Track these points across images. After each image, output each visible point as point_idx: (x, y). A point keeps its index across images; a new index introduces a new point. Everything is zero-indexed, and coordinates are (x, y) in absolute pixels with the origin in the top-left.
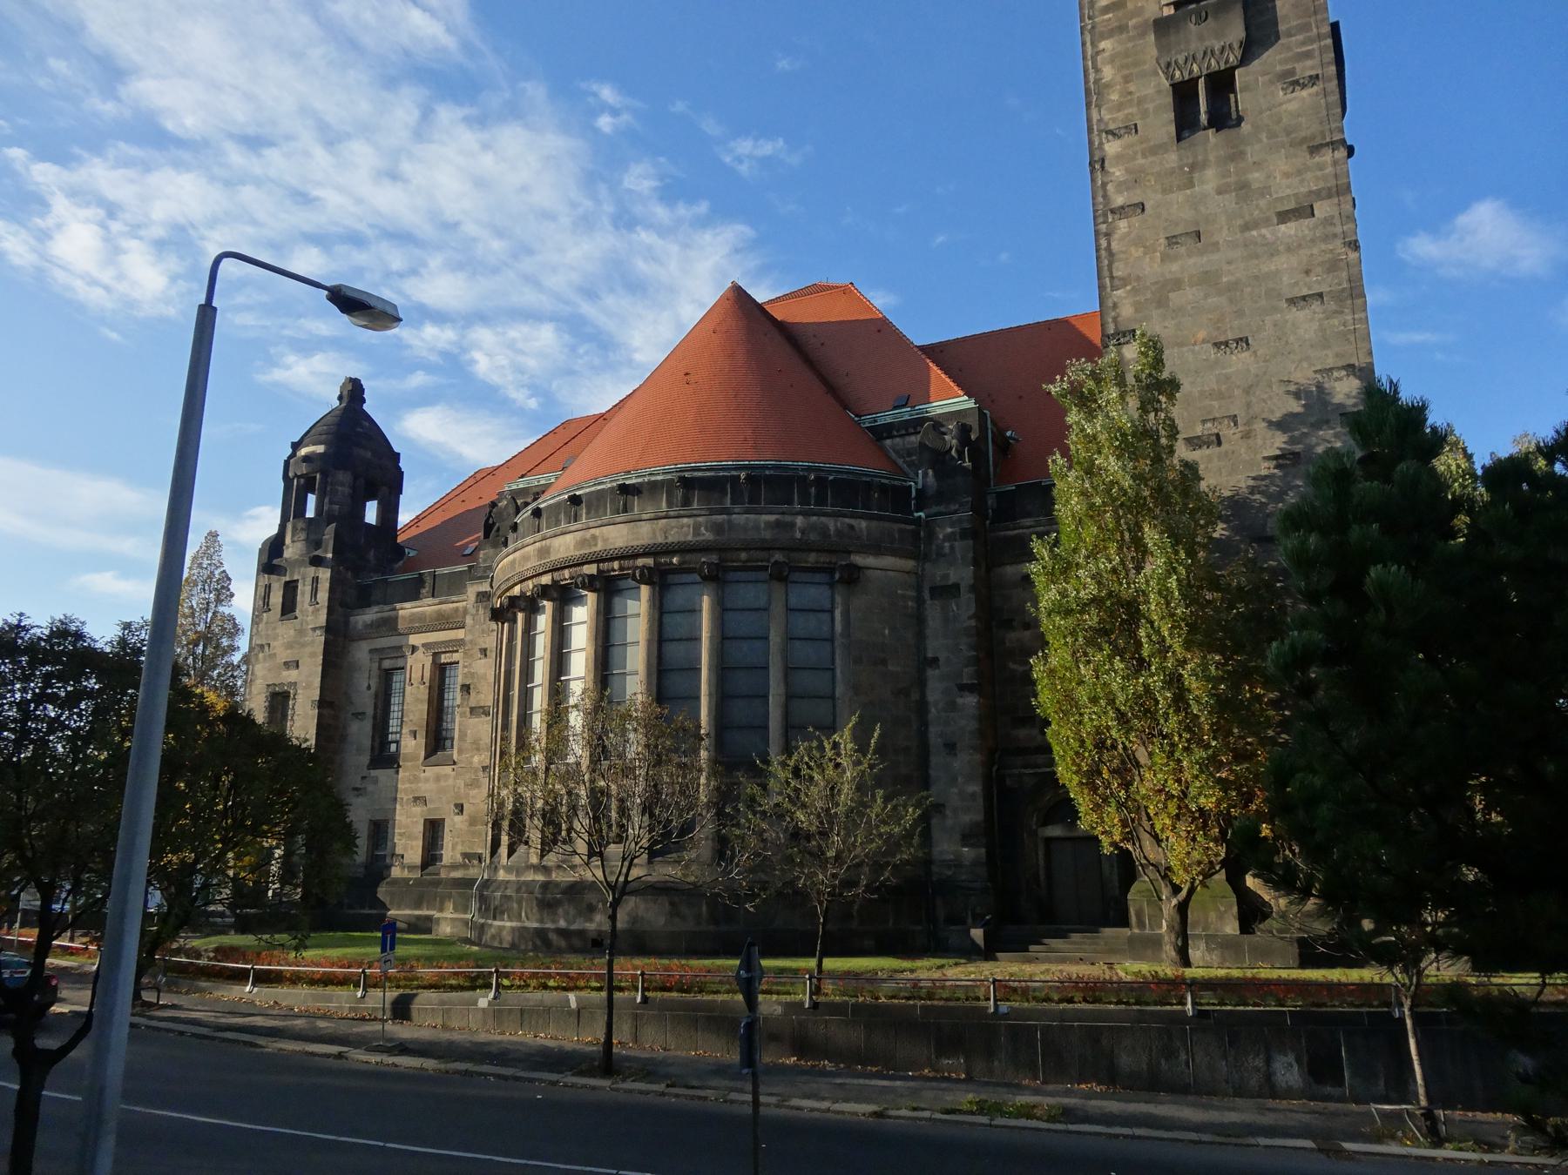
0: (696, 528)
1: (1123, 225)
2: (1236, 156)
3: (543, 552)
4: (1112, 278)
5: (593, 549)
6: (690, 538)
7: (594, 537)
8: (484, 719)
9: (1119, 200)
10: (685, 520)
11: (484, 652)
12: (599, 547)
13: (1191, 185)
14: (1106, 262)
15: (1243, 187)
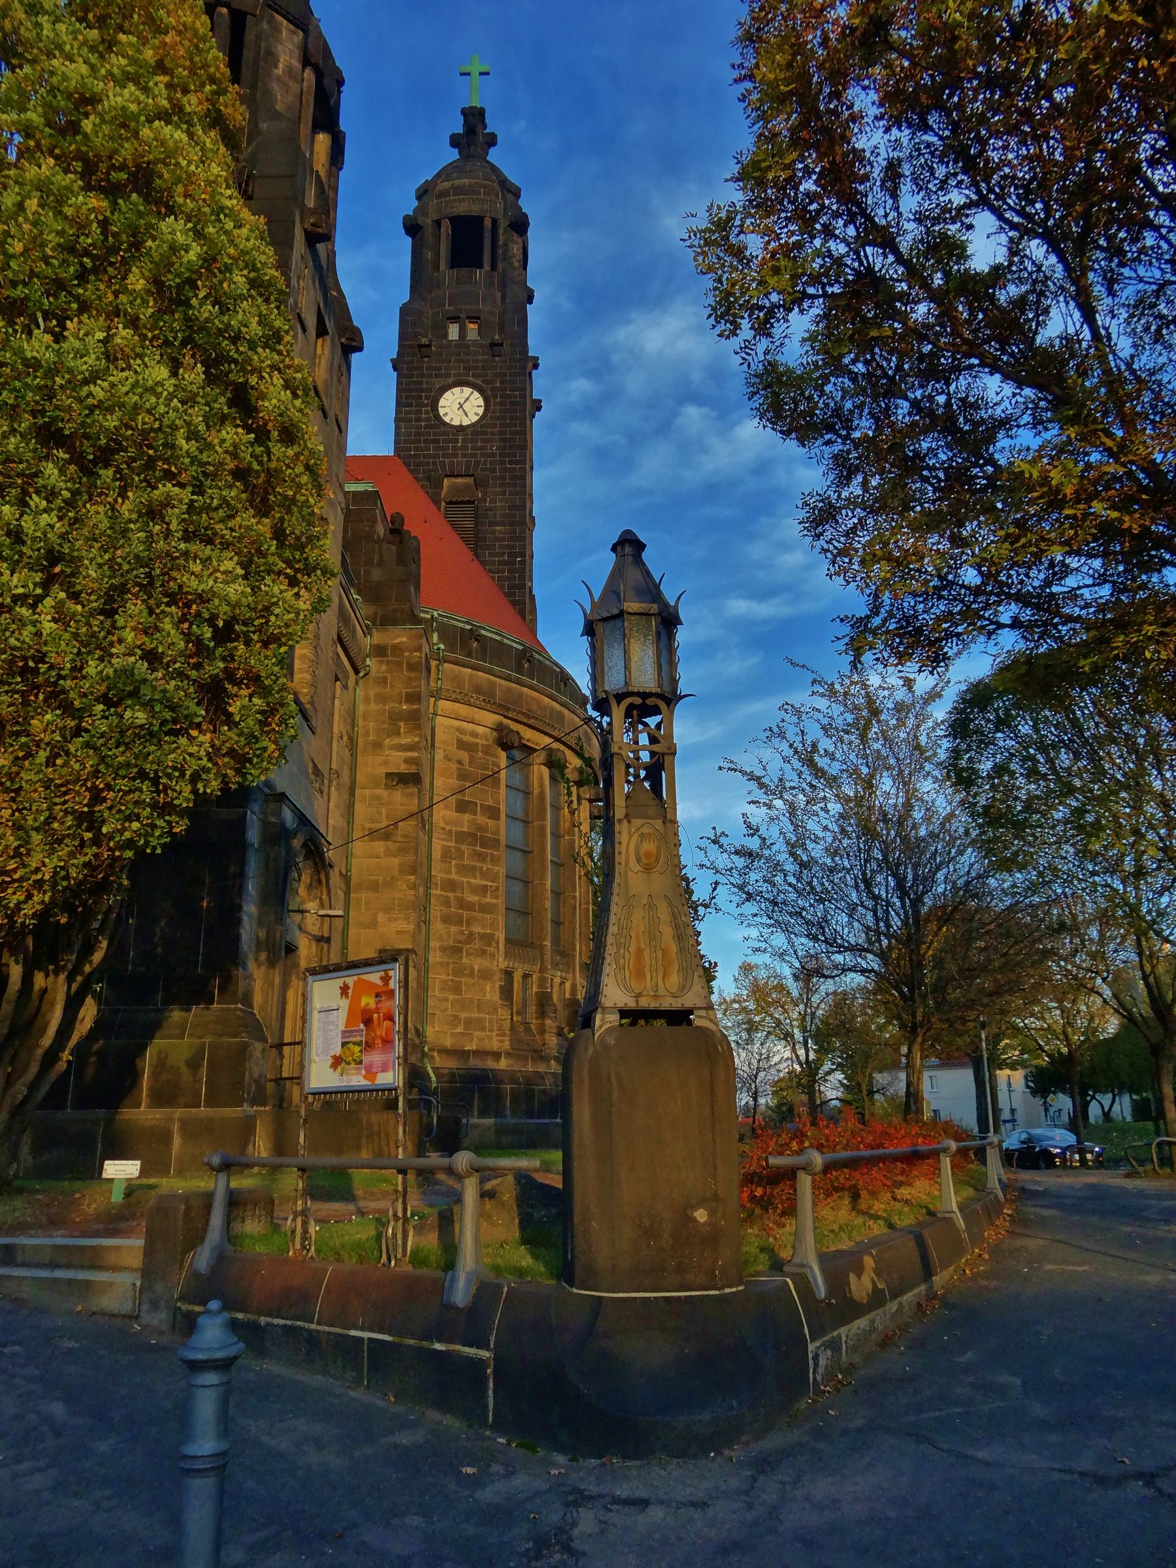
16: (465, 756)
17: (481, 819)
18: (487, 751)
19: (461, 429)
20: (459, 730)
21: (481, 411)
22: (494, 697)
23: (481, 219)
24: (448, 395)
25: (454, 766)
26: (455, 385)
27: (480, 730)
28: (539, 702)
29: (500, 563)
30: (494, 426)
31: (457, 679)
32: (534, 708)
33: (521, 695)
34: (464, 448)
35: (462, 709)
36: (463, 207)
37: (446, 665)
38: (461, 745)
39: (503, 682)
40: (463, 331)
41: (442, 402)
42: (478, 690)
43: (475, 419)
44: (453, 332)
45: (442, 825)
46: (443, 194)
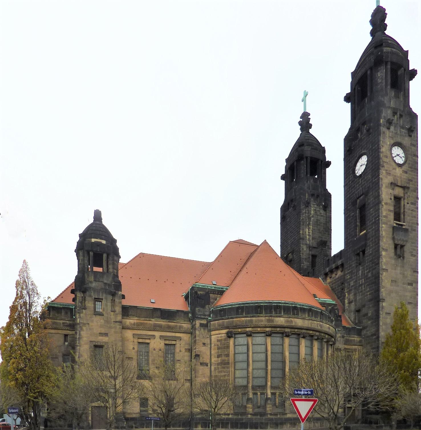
0: (317, 324)
1: (384, 273)
2: (403, 267)
3: (269, 321)
4: (382, 285)
5: (292, 324)
6: (316, 327)
7: (292, 321)
8: (205, 367)
9: (384, 267)
10: (315, 322)
11: (204, 344)
12: (293, 324)
13: (395, 270)
14: (381, 281)
15: (404, 274)
16: (219, 343)
17: (224, 358)
18: (225, 340)
20: (217, 337)
22: (224, 325)
25: (216, 347)
27: (223, 335)
28: (240, 321)
31: (214, 325)
32: (238, 323)
33: (233, 321)
35: (217, 332)
37: (212, 323)
38: (218, 341)
39: (227, 320)
42: (219, 325)
45: (214, 362)
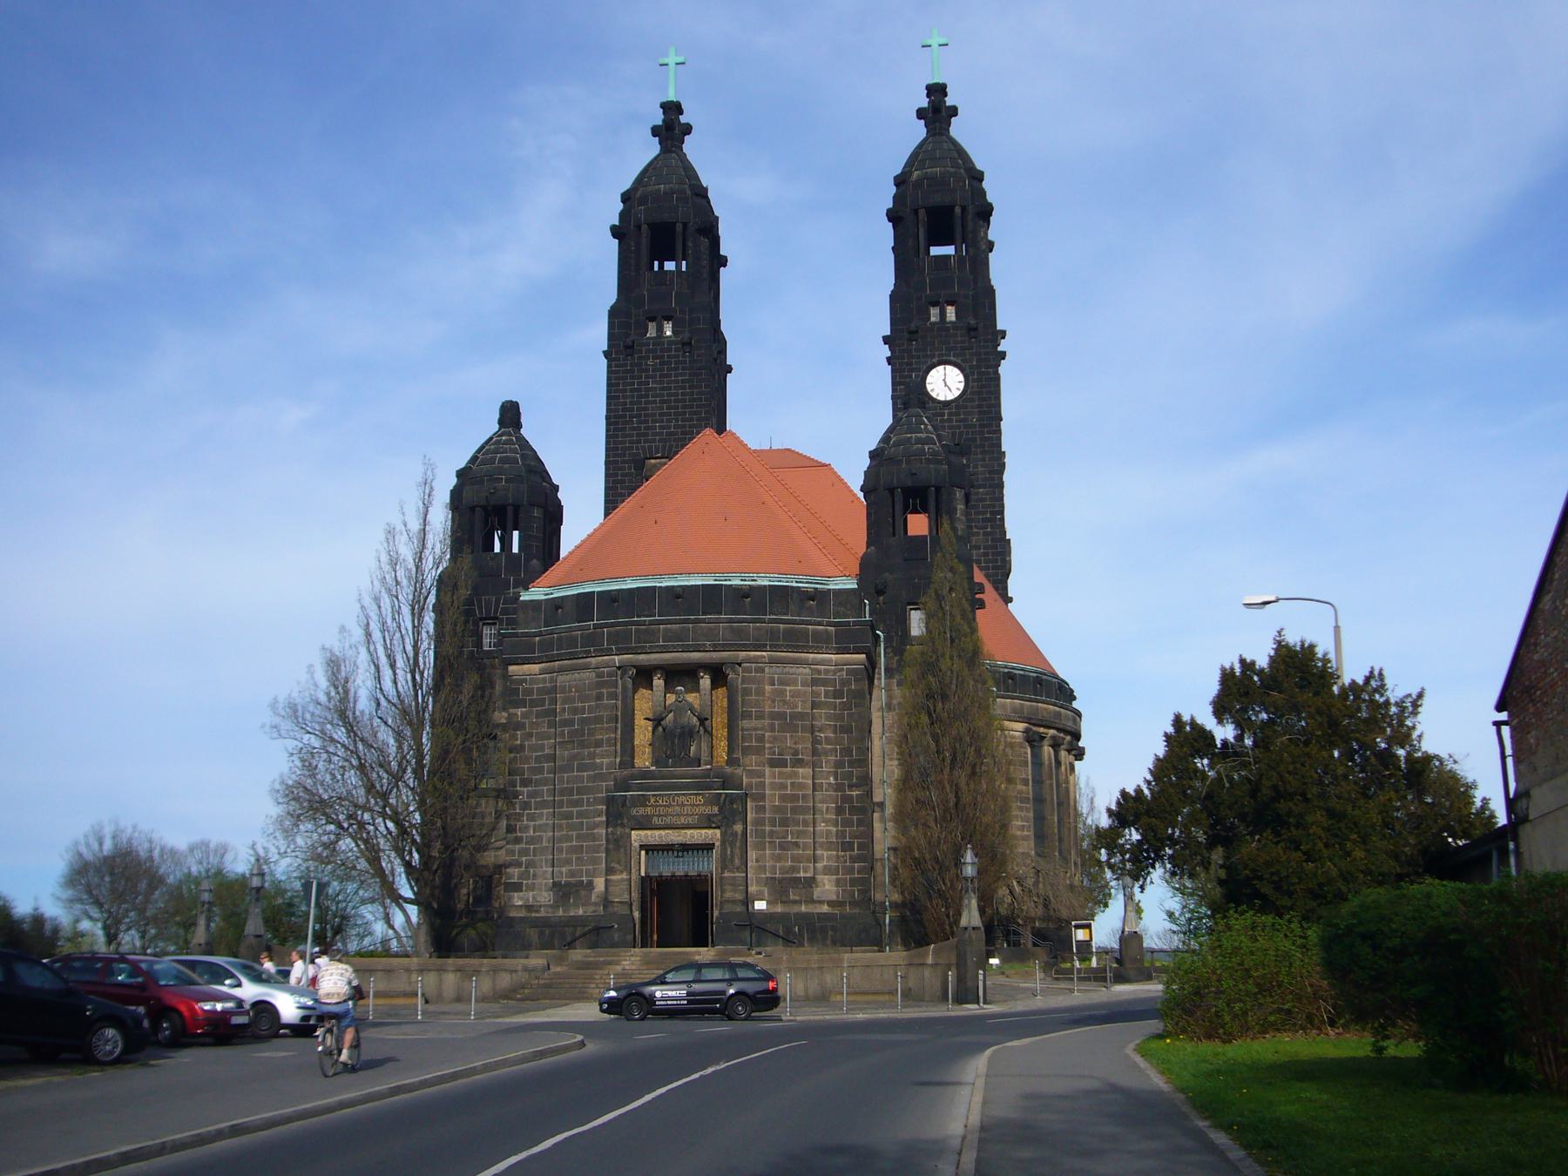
19: (946, 404)
21: (962, 386)
23: (951, 209)
24: (933, 372)
26: (940, 364)
29: (984, 520)
30: (972, 400)
31: (1004, 706)
34: (950, 420)
36: (937, 199)
40: (943, 314)
41: (929, 379)
42: (1014, 710)
43: (957, 393)
44: (934, 313)
46: (918, 184)
